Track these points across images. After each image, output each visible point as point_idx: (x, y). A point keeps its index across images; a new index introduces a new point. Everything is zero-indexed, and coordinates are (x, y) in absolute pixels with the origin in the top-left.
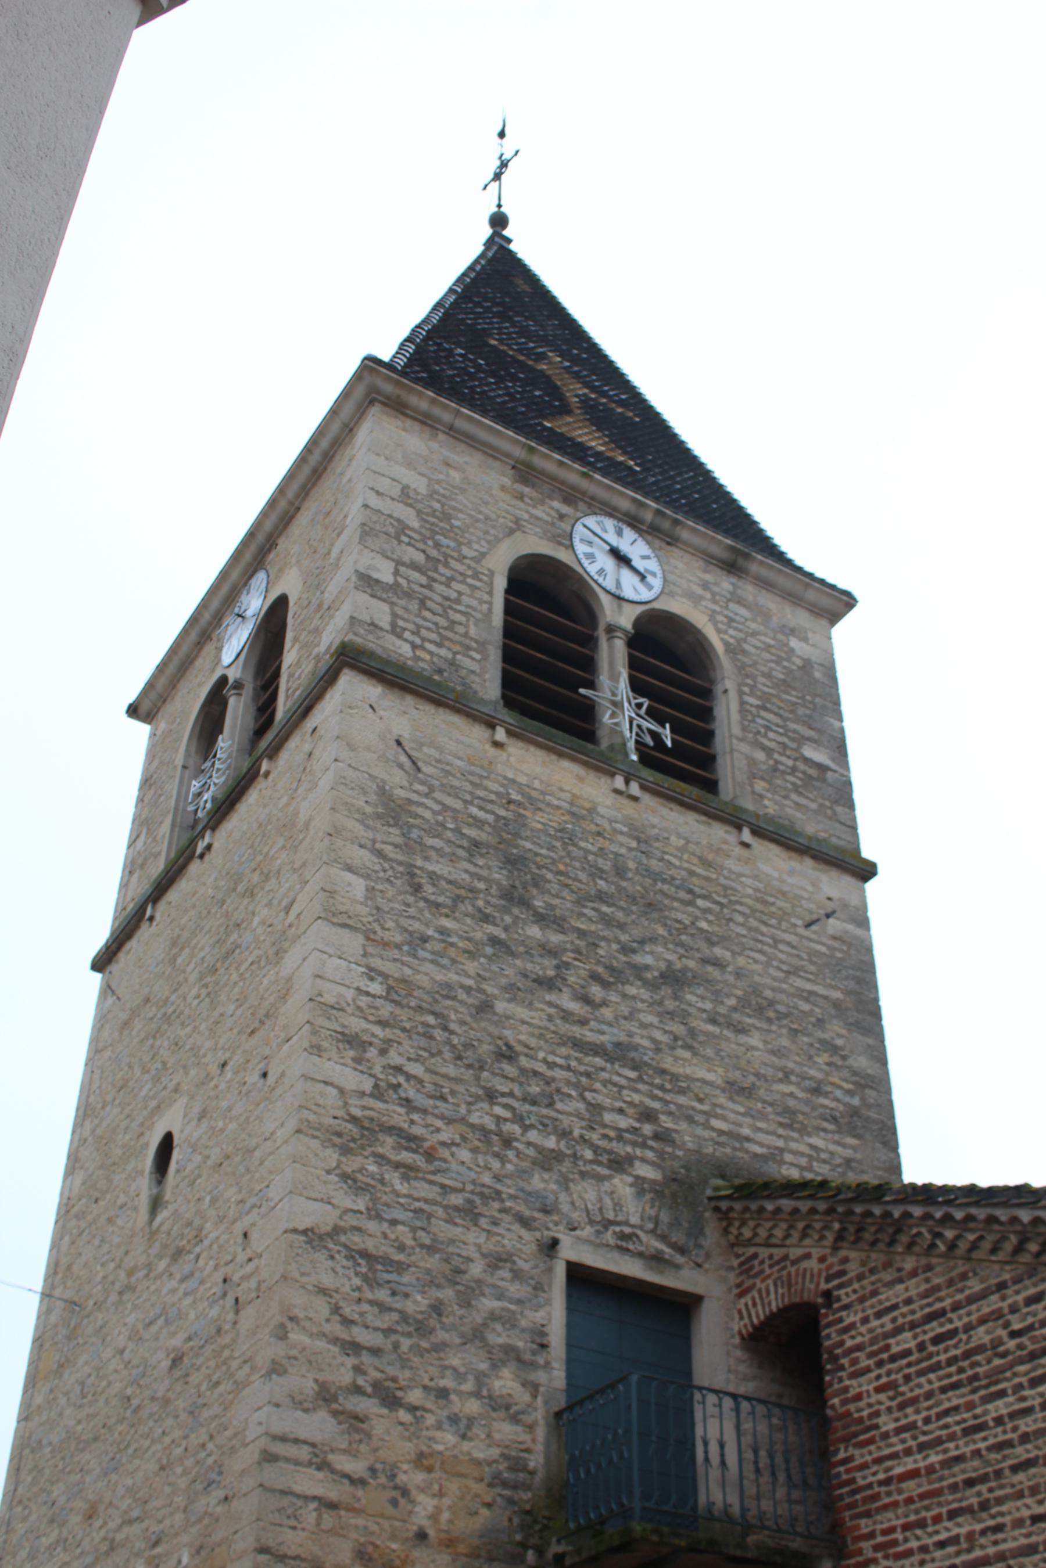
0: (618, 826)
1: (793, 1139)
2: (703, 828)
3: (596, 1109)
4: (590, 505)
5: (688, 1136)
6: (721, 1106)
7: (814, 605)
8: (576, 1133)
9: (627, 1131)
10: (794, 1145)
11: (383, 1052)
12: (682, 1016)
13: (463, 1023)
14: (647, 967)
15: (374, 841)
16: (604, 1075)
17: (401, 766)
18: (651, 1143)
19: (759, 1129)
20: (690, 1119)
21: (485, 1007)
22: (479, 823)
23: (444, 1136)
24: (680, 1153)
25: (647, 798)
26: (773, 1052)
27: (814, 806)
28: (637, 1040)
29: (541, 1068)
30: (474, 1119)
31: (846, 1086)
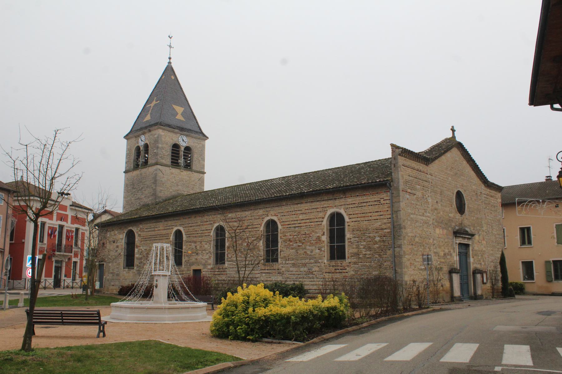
5: (142, 203)
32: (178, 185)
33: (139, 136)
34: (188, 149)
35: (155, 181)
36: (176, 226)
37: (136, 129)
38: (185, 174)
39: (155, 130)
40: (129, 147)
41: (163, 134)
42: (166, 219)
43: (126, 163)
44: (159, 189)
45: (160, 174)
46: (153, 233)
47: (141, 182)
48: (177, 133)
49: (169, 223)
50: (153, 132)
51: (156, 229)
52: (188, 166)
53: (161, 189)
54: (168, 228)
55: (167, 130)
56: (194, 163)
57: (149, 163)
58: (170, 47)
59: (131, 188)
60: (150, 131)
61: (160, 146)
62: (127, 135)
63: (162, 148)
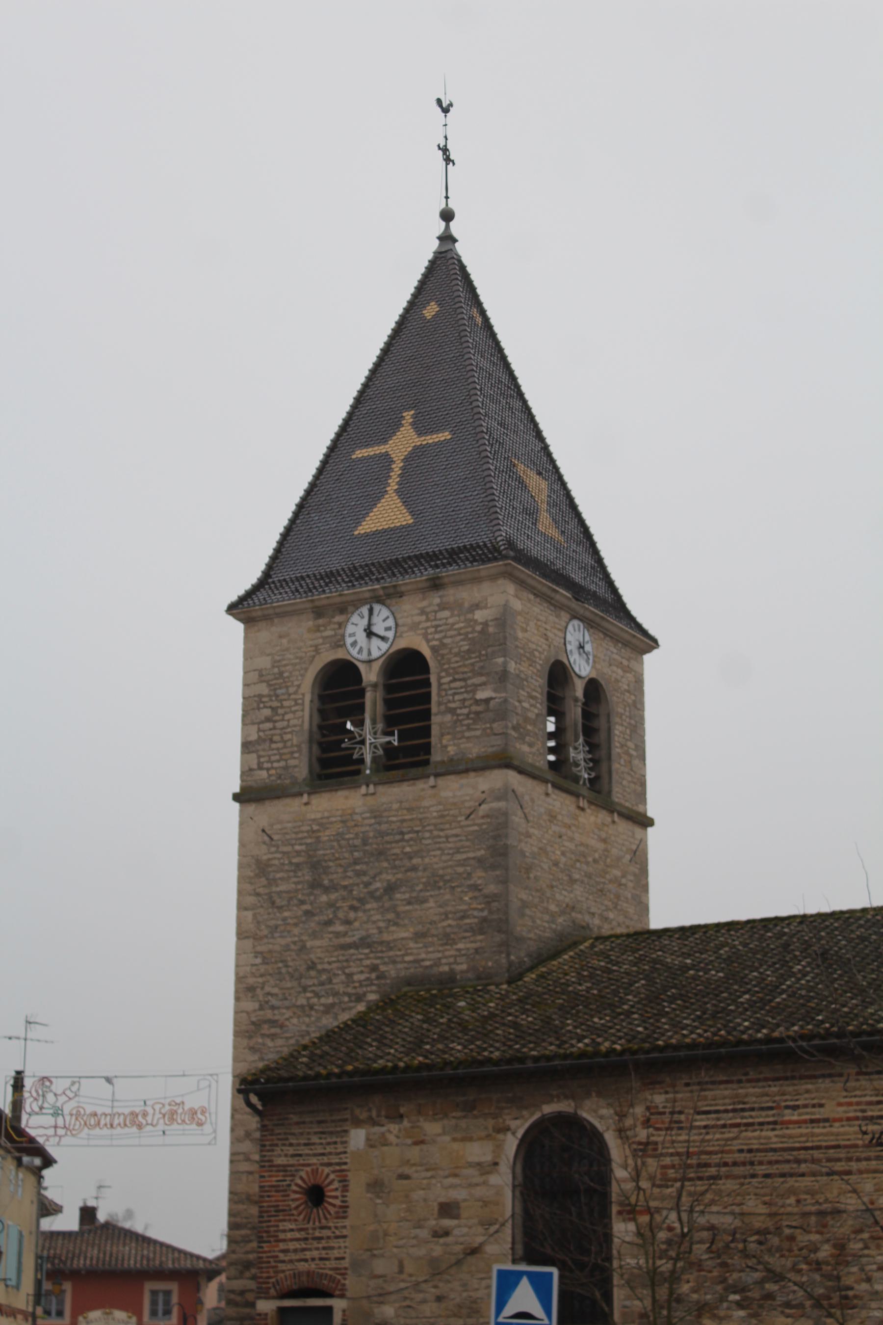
0: (364, 816)
1: (447, 950)
2: (410, 788)
3: (350, 976)
4: (354, 605)
5: (391, 971)
6: (410, 949)
8: (341, 992)
9: (364, 980)
10: (447, 953)
11: (262, 988)
12: (393, 909)
13: (293, 960)
14: (377, 890)
15: (255, 890)
16: (354, 957)
17: (264, 843)
18: (376, 982)
19: (430, 952)
20: (394, 962)
21: (303, 948)
22: (298, 853)
23: (287, 1016)
24: (388, 981)
25: (381, 789)
26: (440, 906)
27: (478, 733)
28: (371, 931)
29: (326, 966)
30: (299, 1003)
31: (479, 907)
32: (572, 881)
33: (345, 609)
39: (477, 580)
43: (246, 746)
44: (518, 894)
45: (517, 819)
46: (771, 1136)
47: (381, 853)
50: (466, 595)
51: (790, 1116)
53: (523, 895)
56: (615, 766)
57: (436, 756)
60: (436, 585)
61: (512, 666)
62: (242, 600)
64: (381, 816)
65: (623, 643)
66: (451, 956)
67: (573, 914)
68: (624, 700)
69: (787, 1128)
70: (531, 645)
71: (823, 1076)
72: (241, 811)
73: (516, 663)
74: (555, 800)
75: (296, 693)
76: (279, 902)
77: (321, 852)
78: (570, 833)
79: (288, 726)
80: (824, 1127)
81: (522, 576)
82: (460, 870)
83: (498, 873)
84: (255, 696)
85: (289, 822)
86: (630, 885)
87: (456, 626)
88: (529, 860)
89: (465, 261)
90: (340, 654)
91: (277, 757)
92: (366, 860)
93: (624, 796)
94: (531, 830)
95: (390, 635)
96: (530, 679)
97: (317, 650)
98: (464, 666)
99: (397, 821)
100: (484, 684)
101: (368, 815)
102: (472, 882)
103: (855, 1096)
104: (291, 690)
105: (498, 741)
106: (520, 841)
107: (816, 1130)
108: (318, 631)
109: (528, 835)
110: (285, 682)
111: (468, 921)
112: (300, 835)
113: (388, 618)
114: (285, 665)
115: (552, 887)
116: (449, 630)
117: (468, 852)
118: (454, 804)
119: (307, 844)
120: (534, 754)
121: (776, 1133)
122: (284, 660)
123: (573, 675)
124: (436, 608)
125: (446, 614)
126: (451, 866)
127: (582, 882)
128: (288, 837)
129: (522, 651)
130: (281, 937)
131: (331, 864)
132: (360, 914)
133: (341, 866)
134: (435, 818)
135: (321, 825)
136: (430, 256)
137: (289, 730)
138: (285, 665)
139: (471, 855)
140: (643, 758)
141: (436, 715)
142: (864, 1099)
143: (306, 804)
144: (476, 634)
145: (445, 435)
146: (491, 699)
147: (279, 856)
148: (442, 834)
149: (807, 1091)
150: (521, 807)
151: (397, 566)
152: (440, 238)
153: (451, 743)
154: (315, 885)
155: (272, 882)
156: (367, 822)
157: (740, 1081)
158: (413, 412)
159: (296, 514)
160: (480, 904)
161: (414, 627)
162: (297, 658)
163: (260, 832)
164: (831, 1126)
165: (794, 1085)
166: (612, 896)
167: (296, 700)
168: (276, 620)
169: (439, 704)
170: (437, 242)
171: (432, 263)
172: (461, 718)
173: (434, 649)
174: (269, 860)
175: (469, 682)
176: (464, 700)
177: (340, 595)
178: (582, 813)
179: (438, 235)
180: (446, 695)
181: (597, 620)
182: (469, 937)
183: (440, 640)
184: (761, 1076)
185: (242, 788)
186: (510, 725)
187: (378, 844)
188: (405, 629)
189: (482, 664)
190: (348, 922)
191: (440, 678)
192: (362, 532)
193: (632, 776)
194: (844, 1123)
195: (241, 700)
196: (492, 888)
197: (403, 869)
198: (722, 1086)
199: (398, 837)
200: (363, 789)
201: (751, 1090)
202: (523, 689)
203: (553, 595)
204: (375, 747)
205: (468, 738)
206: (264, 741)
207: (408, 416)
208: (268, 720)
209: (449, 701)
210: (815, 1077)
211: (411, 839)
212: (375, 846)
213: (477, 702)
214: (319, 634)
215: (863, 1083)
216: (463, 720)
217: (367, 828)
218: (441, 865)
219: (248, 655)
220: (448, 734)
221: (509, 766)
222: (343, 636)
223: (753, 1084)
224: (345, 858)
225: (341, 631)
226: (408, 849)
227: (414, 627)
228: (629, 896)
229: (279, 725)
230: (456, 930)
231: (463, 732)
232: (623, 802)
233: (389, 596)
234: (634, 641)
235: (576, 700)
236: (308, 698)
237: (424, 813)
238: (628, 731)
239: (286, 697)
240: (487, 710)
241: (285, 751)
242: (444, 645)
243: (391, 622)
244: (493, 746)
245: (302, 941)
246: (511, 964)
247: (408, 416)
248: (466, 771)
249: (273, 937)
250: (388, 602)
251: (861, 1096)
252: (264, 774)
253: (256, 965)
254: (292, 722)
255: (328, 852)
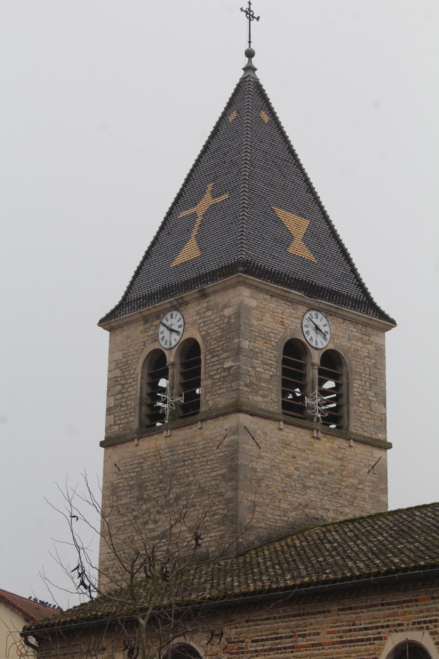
0: (165, 451)
2: (189, 430)
7: (231, 285)
17: (116, 473)
25: (174, 432)
27: (224, 390)
31: (222, 507)
32: (305, 487)
33: (159, 316)
34: (332, 362)
35: (232, 469)
36: (399, 628)
37: (146, 292)
38: (326, 448)
39: (225, 289)
40: (118, 355)
41: (254, 303)
42: (348, 603)
43: (109, 411)
44: (246, 498)
45: (249, 446)
48: (299, 303)
49: (365, 617)
50: (218, 299)
51: (302, 642)
52: (335, 419)
53: (252, 497)
54: (360, 635)
55: (267, 292)
56: (353, 408)
57: (203, 408)
58: (249, 14)
59: (126, 500)
60: (204, 295)
61: (246, 344)
63: (254, 354)
64: (174, 451)
65: (363, 325)
66: (207, 541)
67: (306, 510)
68: (363, 363)
69: (300, 651)
70: (265, 329)
71: (319, 613)
72: (105, 453)
73: (250, 342)
74: (288, 433)
75: (134, 374)
76: (122, 511)
77: (143, 477)
78: (303, 455)
79: (129, 396)
80: (320, 650)
81: (255, 283)
82: (213, 483)
83: (232, 483)
84: (113, 378)
85: (128, 458)
86: (367, 488)
87: (215, 321)
88: (259, 474)
89: (261, 82)
90: (156, 346)
91: (124, 416)
92: (166, 480)
93: (362, 428)
94: (263, 454)
95: (181, 330)
96: (264, 352)
97: (145, 345)
98: (218, 346)
99: (182, 453)
100: (228, 357)
101: (167, 450)
102: (219, 491)
103: (337, 626)
104: (132, 372)
105: (233, 395)
106: (251, 461)
107: (315, 652)
108: (146, 332)
109: (260, 457)
110: (129, 367)
111: (216, 517)
112: (133, 467)
113: (180, 319)
114: (129, 356)
115: (284, 492)
116: (211, 324)
117: (218, 470)
118: (211, 439)
119: (137, 472)
120: (268, 402)
121: (293, 654)
122: (128, 352)
123: (309, 347)
124: (205, 310)
125: (210, 313)
126: (209, 481)
127: (317, 488)
128: (127, 468)
129: (257, 334)
130: (122, 534)
131: (148, 484)
132: (162, 516)
133: (153, 485)
134: (201, 449)
135: (144, 458)
136: (238, 81)
137: (130, 398)
138: (129, 356)
139: (219, 472)
140: (384, 402)
141: (203, 380)
142: (341, 628)
143: (137, 445)
144: (225, 325)
145: (226, 196)
146: (232, 366)
147: (122, 480)
148: (204, 459)
149: (311, 624)
150: (253, 438)
151: (187, 285)
152: (245, 69)
153: (210, 398)
154: (140, 499)
155: (119, 498)
156: (167, 455)
157: (275, 618)
158: (211, 185)
159: (146, 258)
160: (222, 505)
161: (193, 323)
162: (135, 351)
163: (114, 466)
164: (323, 649)
165: (304, 619)
166: (348, 497)
167: (134, 378)
168: (125, 327)
169: (205, 373)
170: (243, 72)
171: (239, 86)
172: (215, 381)
173: (203, 337)
174: (118, 483)
175: (221, 357)
176: (218, 369)
177: (154, 307)
178: (318, 441)
179: (244, 66)
180: (209, 367)
181: (333, 309)
182: (217, 528)
183: (206, 331)
184: (286, 614)
185: (106, 438)
186: (243, 383)
187: (171, 469)
188: (189, 325)
189: (227, 344)
190: (156, 522)
191: (206, 355)
192: (174, 265)
193: (371, 414)
194: (331, 646)
195: (107, 381)
196: (229, 494)
197: (184, 484)
198: (265, 622)
199: (182, 464)
200: (165, 434)
201: (281, 624)
202: (257, 359)
203: (287, 295)
204: (172, 405)
205: (220, 394)
206: (117, 406)
207: (210, 187)
208: (120, 392)
209: (210, 371)
210: (314, 613)
211: (189, 464)
212: (170, 470)
213: (225, 370)
214: (146, 334)
215: (342, 616)
216: (217, 382)
217: (167, 459)
218: (204, 480)
219: (111, 352)
220: (209, 392)
221: (239, 411)
222: (158, 334)
223: (282, 620)
224: (155, 480)
225: (157, 331)
226: (187, 471)
227: (193, 323)
228: (367, 496)
229: (126, 395)
230: (210, 524)
231: (216, 390)
232: (362, 433)
233: (181, 305)
234: (372, 323)
235: (313, 365)
236: (140, 376)
237: (196, 446)
238: (367, 384)
239: (128, 377)
240: (229, 375)
241: (127, 412)
242: (208, 334)
243: (181, 322)
244: (231, 399)
245: (132, 536)
246: (239, 545)
247: (210, 187)
248: (217, 416)
249: (118, 535)
250: (181, 308)
251: (340, 627)
252: (117, 427)
253: (109, 553)
254: (132, 393)
255: (147, 476)
